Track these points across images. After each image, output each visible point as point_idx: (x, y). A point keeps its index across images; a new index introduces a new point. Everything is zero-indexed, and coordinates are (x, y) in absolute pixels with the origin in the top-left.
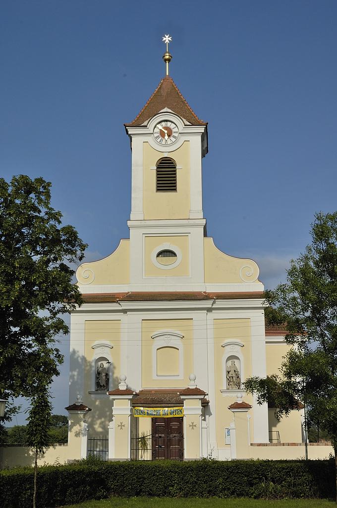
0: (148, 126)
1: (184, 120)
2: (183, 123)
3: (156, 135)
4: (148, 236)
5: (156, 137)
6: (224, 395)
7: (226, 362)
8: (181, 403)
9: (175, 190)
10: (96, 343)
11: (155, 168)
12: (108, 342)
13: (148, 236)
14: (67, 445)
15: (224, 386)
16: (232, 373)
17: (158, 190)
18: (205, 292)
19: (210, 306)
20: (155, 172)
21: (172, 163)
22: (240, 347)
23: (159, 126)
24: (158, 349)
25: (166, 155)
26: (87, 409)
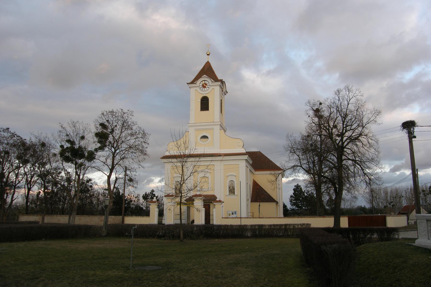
0: (197, 83)
1: (212, 80)
2: (211, 81)
3: (200, 87)
4: (197, 130)
5: (200, 88)
6: (228, 197)
7: (229, 181)
8: (193, 200)
9: (208, 110)
10: (229, 174)
11: (200, 101)
12: (234, 174)
13: (197, 130)
14: (149, 217)
15: (228, 193)
16: (231, 188)
17: (208, 110)
18: (220, 153)
19: (221, 159)
20: (200, 102)
21: (207, 98)
22: (234, 177)
23: (202, 83)
24: (200, 178)
25: (204, 95)
26: (222, 202)
